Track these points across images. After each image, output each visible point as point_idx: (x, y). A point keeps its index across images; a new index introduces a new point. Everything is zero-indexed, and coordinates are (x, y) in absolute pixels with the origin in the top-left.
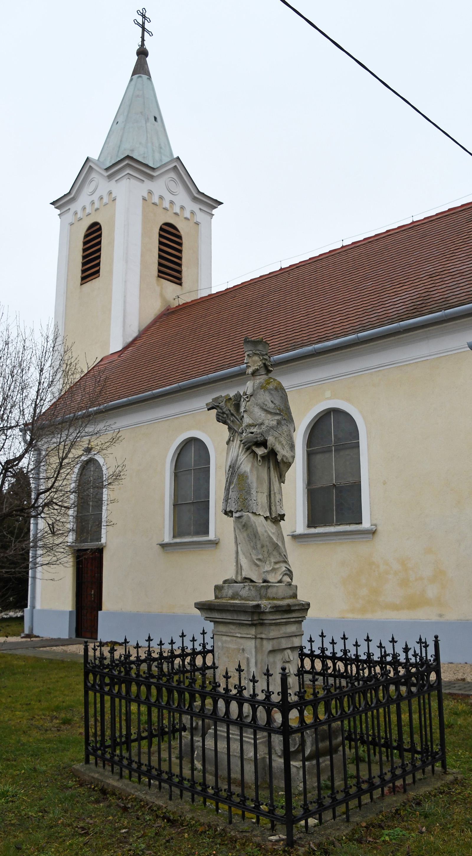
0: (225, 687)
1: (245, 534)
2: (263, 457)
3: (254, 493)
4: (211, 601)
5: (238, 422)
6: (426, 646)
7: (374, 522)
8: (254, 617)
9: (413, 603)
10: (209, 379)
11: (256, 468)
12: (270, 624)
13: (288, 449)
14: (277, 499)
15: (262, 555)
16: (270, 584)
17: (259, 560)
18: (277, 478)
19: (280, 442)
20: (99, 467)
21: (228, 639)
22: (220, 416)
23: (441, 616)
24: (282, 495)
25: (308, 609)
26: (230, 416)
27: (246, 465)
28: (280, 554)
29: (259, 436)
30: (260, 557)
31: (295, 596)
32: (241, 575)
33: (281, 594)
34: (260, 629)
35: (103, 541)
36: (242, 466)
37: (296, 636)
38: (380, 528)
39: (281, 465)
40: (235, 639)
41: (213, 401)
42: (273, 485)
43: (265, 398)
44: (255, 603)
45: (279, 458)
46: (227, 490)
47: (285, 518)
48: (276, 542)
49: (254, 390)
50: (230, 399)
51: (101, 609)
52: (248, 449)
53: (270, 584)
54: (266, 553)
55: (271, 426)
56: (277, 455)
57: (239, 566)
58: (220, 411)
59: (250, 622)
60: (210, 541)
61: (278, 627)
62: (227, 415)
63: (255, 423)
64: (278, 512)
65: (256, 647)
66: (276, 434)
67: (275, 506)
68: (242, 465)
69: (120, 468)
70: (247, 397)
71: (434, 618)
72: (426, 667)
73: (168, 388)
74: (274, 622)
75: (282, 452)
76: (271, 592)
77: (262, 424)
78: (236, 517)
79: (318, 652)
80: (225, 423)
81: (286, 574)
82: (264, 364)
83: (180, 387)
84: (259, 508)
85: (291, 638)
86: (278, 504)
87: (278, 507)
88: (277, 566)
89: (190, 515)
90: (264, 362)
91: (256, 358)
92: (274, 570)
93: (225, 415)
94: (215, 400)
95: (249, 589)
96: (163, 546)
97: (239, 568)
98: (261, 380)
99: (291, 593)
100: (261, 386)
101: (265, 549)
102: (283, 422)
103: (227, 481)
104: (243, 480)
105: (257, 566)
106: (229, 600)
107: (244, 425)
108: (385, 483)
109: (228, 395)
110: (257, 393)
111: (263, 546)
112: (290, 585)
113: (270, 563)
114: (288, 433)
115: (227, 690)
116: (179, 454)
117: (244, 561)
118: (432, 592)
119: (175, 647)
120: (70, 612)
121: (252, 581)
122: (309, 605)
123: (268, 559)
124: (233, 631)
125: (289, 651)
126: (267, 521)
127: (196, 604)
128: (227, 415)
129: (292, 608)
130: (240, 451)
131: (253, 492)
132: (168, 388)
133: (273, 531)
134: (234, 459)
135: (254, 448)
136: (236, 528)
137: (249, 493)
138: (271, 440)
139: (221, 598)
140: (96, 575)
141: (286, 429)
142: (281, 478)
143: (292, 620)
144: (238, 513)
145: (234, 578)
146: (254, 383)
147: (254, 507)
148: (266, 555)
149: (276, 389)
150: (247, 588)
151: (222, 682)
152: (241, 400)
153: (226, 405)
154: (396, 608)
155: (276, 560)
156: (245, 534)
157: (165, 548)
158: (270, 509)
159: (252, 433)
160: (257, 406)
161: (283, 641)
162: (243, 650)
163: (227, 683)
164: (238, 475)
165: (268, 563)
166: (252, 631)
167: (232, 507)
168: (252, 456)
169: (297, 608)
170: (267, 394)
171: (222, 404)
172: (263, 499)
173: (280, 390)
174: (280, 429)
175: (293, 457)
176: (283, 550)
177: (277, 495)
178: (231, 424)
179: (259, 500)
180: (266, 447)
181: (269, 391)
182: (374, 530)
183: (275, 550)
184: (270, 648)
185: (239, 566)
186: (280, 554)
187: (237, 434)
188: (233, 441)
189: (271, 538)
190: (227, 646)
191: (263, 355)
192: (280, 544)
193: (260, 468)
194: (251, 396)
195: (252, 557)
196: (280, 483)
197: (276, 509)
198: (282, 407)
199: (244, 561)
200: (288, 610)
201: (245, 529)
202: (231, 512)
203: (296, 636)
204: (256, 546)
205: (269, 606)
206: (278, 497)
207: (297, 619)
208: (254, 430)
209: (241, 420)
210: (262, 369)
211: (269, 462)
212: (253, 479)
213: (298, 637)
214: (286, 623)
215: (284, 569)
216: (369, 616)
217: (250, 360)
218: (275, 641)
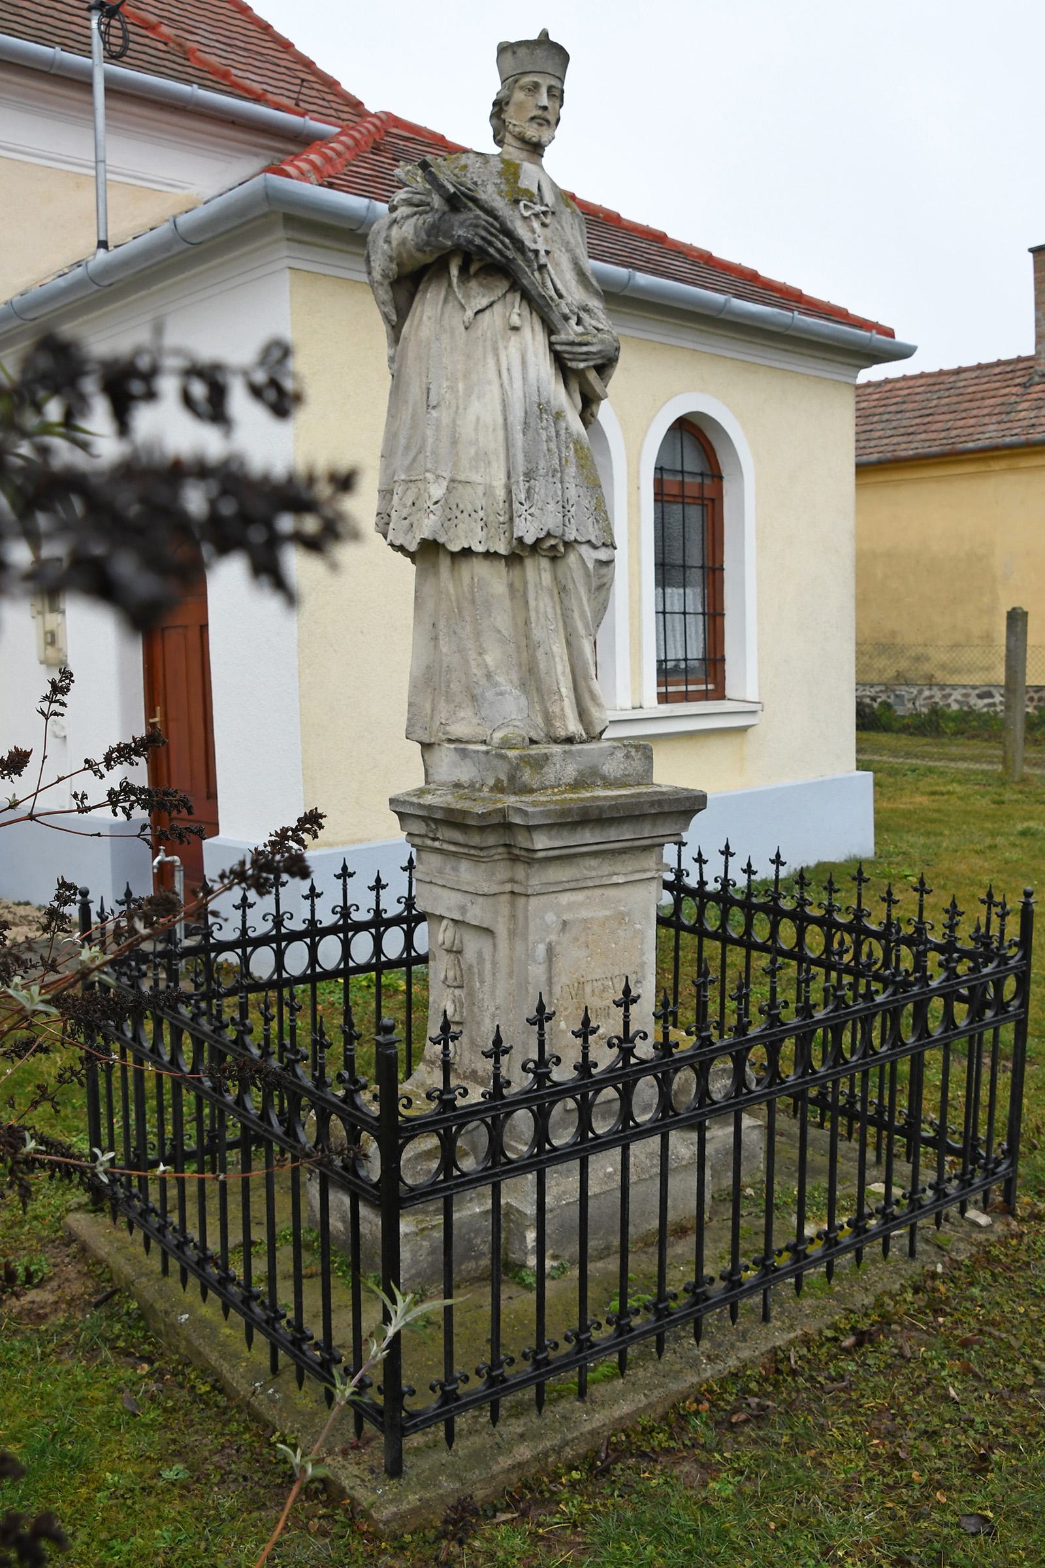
21: (579, 897)
40: (598, 892)
95: (627, 756)
124: (593, 873)
144: (604, 549)
160: (567, 251)
194: (553, 213)
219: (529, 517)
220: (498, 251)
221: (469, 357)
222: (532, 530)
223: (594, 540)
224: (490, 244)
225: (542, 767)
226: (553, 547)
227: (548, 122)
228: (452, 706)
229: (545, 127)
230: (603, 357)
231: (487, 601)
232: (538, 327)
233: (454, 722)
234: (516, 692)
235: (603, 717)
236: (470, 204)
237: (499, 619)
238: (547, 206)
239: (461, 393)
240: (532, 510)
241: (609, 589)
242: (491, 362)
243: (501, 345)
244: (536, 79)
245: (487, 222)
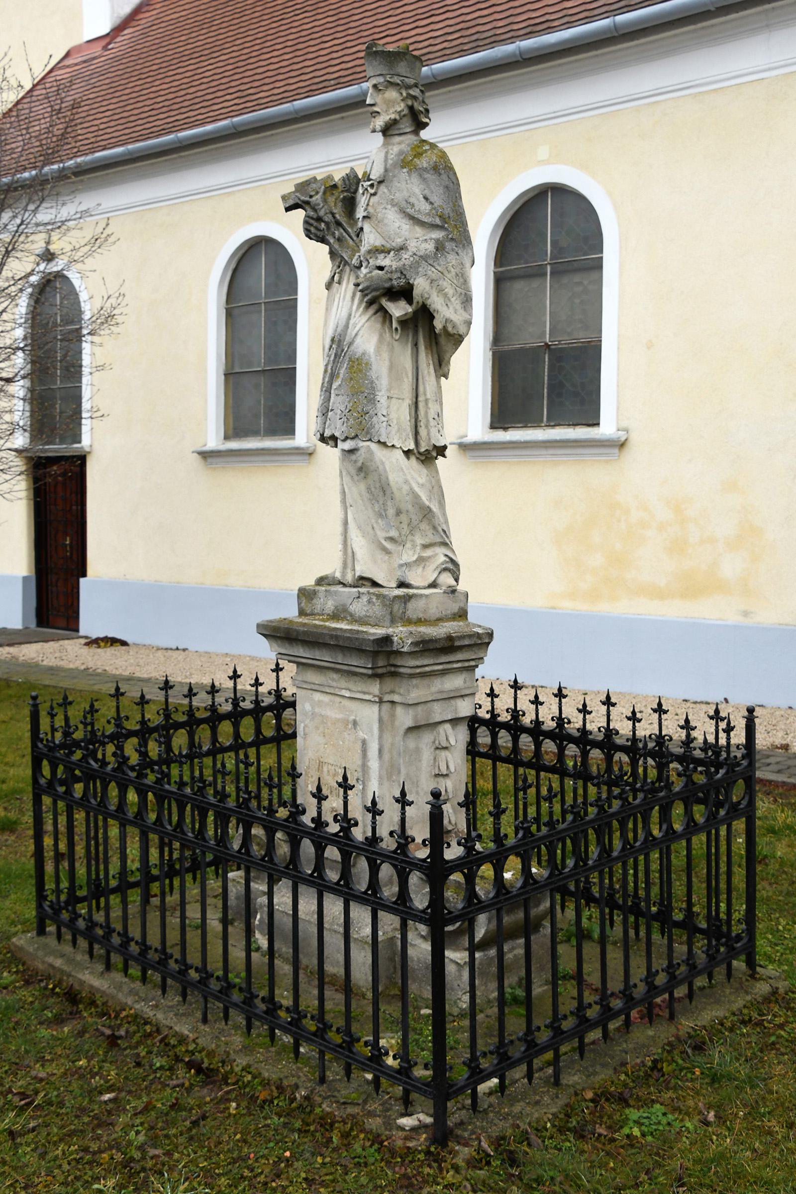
0: (315, 814)
1: (362, 486)
2: (404, 323)
3: (382, 401)
4: (291, 622)
5: (351, 242)
6: (729, 730)
7: (624, 424)
8: (380, 661)
9: (692, 587)
10: (296, 112)
11: (389, 344)
12: (411, 675)
13: (459, 306)
14: (432, 413)
15: (398, 529)
16: (411, 591)
17: (391, 539)
18: (432, 367)
19: (441, 290)
20: (72, 294)
21: (326, 698)
22: (311, 225)
23: (746, 614)
24: (441, 404)
25: (489, 643)
26: (333, 226)
27: (367, 337)
28: (435, 528)
29: (395, 276)
30: (393, 533)
31: (462, 614)
32: (354, 570)
33: (434, 611)
34: (389, 684)
35: (86, 441)
36: (358, 341)
37: (462, 696)
38: (635, 437)
39: (443, 340)
40: (338, 699)
41: (297, 191)
42: (424, 384)
43: (410, 188)
44: (380, 632)
45: (438, 324)
46: (327, 390)
47: (447, 452)
48: (427, 503)
49: (386, 170)
50: (335, 186)
51: (84, 574)
52: (370, 303)
53: (411, 591)
54: (404, 525)
55: (421, 253)
56: (433, 317)
57: (349, 551)
58: (312, 213)
59: (370, 672)
60: (297, 448)
61: (426, 681)
62: (327, 224)
63: (388, 246)
64: (433, 442)
65: (381, 720)
66: (432, 272)
67: (427, 427)
68: (359, 337)
69: (112, 301)
70: (372, 186)
71: (733, 618)
72: (727, 773)
73: (209, 127)
74: (418, 670)
75: (445, 312)
76: (414, 609)
77: (402, 248)
78: (343, 450)
79: (505, 717)
80: (322, 240)
81: (445, 569)
82: (411, 108)
83: (234, 126)
84: (393, 432)
85: (453, 702)
86: (432, 423)
87: (433, 431)
88: (428, 553)
89: (258, 396)
90: (410, 103)
91: (392, 94)
92: (421, 560)
93: (323, 225)
94: (302, 187)
95: (369, 602)
96: (206, 455)
97: (349, 557)
98: (403, 146)
99: (455, 607)
100: (403, 161)
101: (403, 518)
102: (449, 245)
103: (326, 371)
104: (361, 371)
105: (387, 552)
106: (328, 620)
107: (363, 249)
109: (330, 177)
110: (394, 176)
111: (398, 513)
112: (454, 591)
113: (414, 546)
114: (458, 270)
115: (319, 821)
116: (235, 271)
117: (358, 543)
118: (731, 566)
119: (220, 699)
120: (25, 579)
121: (375, 584)
122: (491, 635)
123: (410, 537)
124: (334, 684)
125: (448, 726)
126: (408, 458)
127: (258, 626)
128: (327, 224)
129: (457, 643)
130: (355, 307)
131: (382, 397)
132: (209, 127)
133: (421, 481)
134: (342, 323)
135: (384, 302)
136: (344, 473)
137: (372, 400)
138: (421, 285)
139: (312, 614)
140: (74, 507)
141: (454, 262)
142: (441, 367)
143: (455, 666)
145: (338, 575)
146: (387, 153)
147: (383, 431)
148: (405, 530)
149: (435, 169)
150: (365, 599)
151: (311, 805)
152: (356, 190)
153: (325, 201)
154: (660, 594)
155: (427, 541)
156: (362, 486)
157: (209, 460)
158: (416, 434)
159: (381, 268)
160: (393, 206)
161: (436, 707)
162: (355, 723)
163: (319, 808)
164: (350, 360)
165: (408, 545)
166: (375, 688)
167: (337, 428)
168: (381, 319)
169: (467, 642)
170: (415, 179)
171: (317, 199)
172: (401, 412)
173: (443, 170)
174: (442, 261)
175: (469, 323)
176: (442, 520)
177: (430, 405)
178: (336, 246)
179: (393, 415)
180: (410, 300)
181: (421, 172)
182: (623, 439)
183: (426, 520)
184: (409, 723)
185: (349, 551)
186: (435, 528)
187: (347, 269)
188: (339, 283)
189: (416, 496)
190: (323, 713)
191: (408, 87)
192: (435, 508)
193: (396, 344)
194: (380, 182)
195: (375, 535)
196: (438, 378)
197: (428, 434)
198: (447, 211)
199: (358, 543)
200: (449, 646)
201: (362, 475)
202: (334, 438)
203: (462, 696)
204: (385, 510)
205: (409, 642)
206: (433, 408)
207: (466, 664)
208: (386, 261)
209: (358, 236)
210: (405, 119)
211: (416, 333)
212: (380, 370)
213: (466, 699)
214: (444, 673)
215: (443, 559)
216: (604, 607)
217: (379, 99)
218: (420, 708)
225: (312, 599)
227: (378, 113)
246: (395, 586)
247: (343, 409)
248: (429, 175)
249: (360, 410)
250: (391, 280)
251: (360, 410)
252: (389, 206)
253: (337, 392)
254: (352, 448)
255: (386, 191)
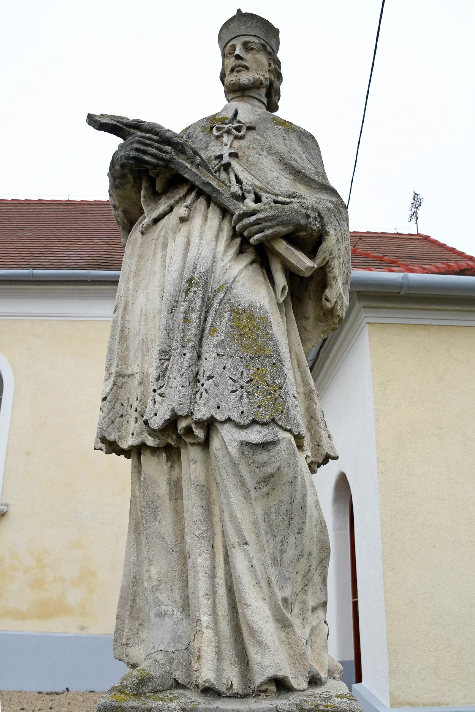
9: (46, 610)
23: (82, 628)
38: (12, 510)
70: (238, 129)
71: (73, 631)
101: (302, 565)
108: (28, 454)
118: (74, 597)
123: (300, 597)
154: (21, 616)
156: (259, 511)
182: (5, 511)
194: (250, 128)
201: (265, 489)
219: (158, 398)
220: (153, 155)
221: (141, 256)
222: (161, 412)
223: (235, 416)
224: (145, 152)
226: (189, 431)
227: (247, 68)
228: (137, 623)
229: (242, 72)
230: (283, 224)
231: (153, 502)
232: (214, 216)
233: (134, 644)
234: (178, 614)
235: (266, 662)
236: (133, 131)
237: (164, 523)
238: (239, 122)
239: (130, 291)
240: (163, 389)
241: (292, 483)
242: (159, 255)
243: (169, 240)
244: (232, 43)
245: (141, 137)
246: (305, 685)
247: (237, 377)
248: (307, 140)
249: (270, 381)
250: (308, 216)
251: (270, 381)
252: (265, 154)
253: (219, 351)
254: (269, 439)
255: (258, 137)
